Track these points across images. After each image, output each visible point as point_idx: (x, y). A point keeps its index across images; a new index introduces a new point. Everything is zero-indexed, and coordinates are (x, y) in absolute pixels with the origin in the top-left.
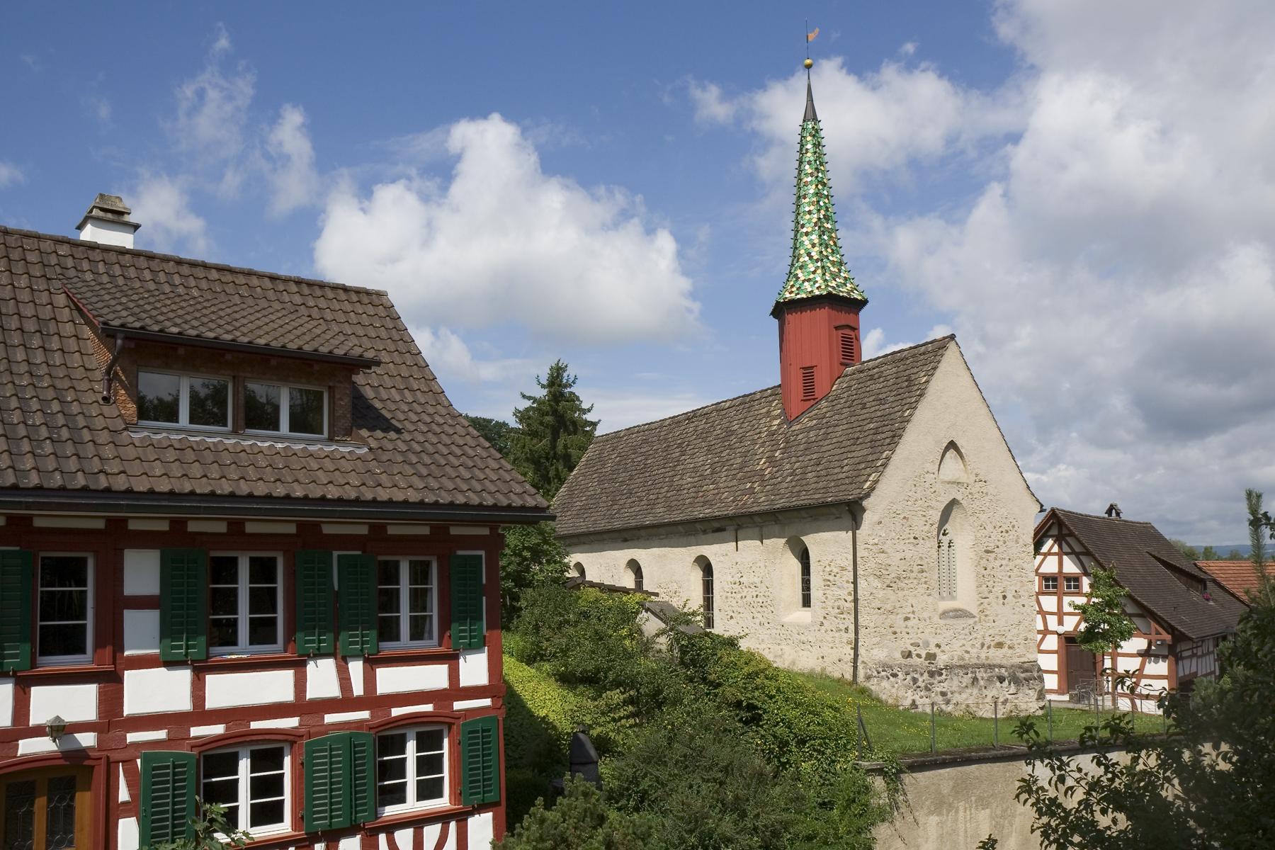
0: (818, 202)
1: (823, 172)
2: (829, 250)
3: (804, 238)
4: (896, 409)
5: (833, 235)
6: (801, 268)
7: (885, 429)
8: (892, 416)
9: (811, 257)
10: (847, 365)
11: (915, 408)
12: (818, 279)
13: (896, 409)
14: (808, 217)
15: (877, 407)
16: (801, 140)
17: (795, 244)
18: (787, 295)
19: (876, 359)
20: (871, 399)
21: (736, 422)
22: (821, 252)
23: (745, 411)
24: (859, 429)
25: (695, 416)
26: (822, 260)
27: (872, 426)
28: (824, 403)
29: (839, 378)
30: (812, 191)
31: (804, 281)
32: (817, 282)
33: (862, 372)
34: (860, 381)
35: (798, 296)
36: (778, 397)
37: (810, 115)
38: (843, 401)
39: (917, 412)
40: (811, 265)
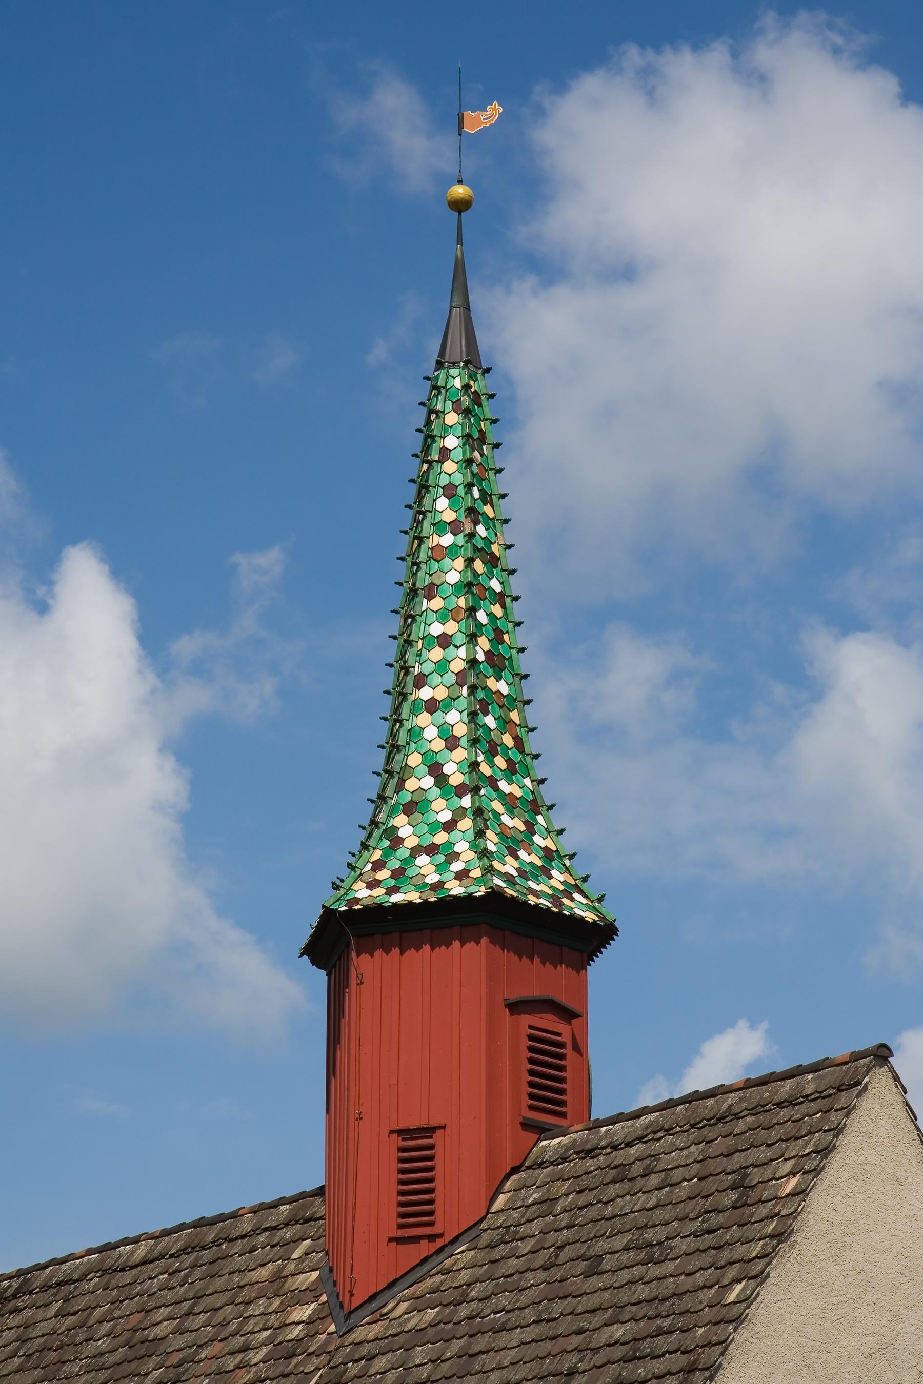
0: (472, 611)
1: (489, 523)
2: (500, 761)
3: (424, 719)
4: (699, 1278)
5: (514, 716)
6: (409, 809)
7: (663, 1343)
8: (687, 1302)
9: (441, 779)
10: (543, 1131)
11: (761, 1278)
12: (462, 847)
13: (699, 1278)
14: (437, 654)
15: (637, 1271)
16: (428, 423)
17: (393, 735)
18: (362, 892)
19: (636, 1115)
20: (619, 1242)
21: (164, 1312)
22: (475, 765)
23: (198, 1273)
24: (576, 1340)
25: (24, 1290)
26: (476, 790)
27: (618, 1332)
28: (463, 1254)
29: (515, 1170)
30: (453, 577)
31: (415, 851)
32: (456, 856)
33: (590, 1153)
34: (584, 1182)
35: (397, 898)
36: (313, 1229)
37: (457, 347)
38: (525, 1247)
39: (768, 1292)
40: (439, 804)
